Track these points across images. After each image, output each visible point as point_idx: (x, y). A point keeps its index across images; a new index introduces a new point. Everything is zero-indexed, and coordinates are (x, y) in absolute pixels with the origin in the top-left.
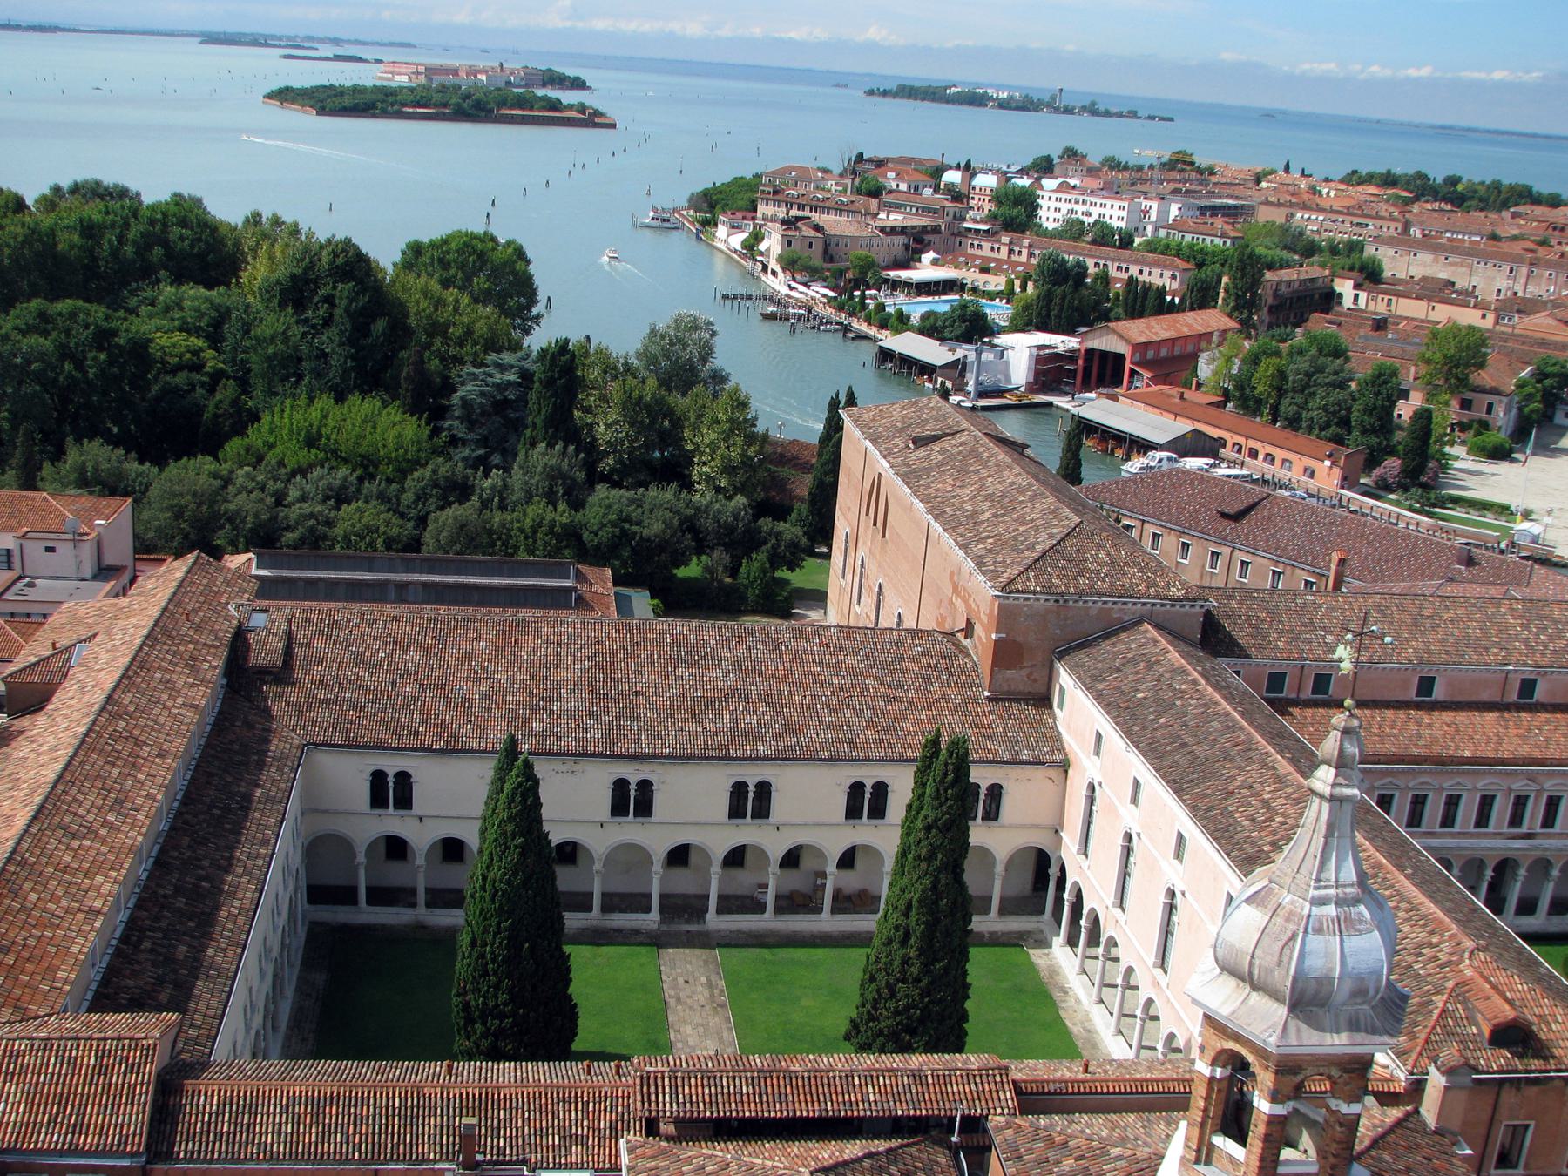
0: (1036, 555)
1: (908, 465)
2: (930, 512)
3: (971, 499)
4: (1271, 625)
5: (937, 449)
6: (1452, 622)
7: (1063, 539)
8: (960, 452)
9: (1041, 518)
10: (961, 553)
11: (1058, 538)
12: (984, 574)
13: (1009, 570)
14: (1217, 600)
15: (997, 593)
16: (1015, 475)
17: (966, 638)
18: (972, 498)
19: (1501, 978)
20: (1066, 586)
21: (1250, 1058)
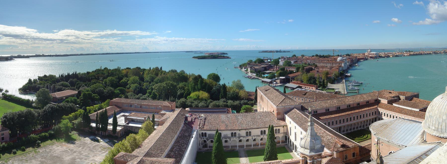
0: (280, 102)
2: (268, 98)
7: (284, 100)
10: (272, 103)
19: (341, 140)
21: (306, 156)
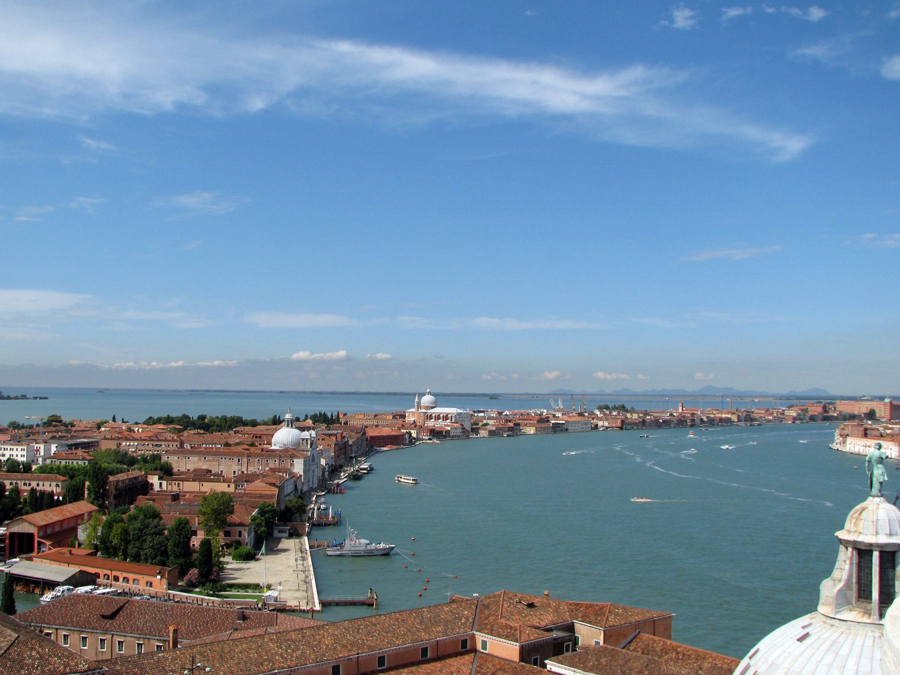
6: (241, 652)
7: (8, 649)
11: (5, 648)
14: (107, 667)
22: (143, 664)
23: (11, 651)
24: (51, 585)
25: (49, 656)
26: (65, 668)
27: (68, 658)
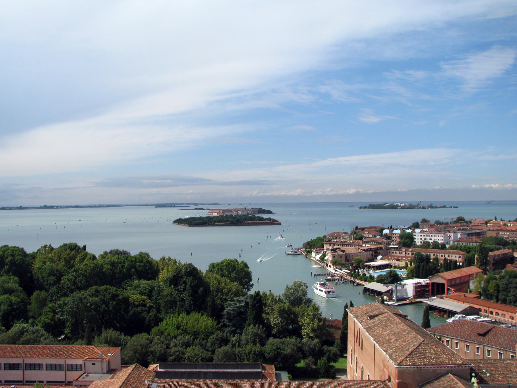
0: (409, 352)
1: (368, 325)
2: (374, 340)
3: (388, 335)
4: (495, 372)
5: (377, 319)
7: (418, 346)
8: (384, 320)
9: (411, 340)
10: (385, 353)
11: (417, 346)
12: (392, 360)
13: (400, 358)
14: (475, 364)
15: (396, 366)
16: (402, 326)
17: (389, 382)
18: (388, 335)
20: (420, 362)
22: (497, 365)
23: (420, 348)
24: (452, 313)
25: (441, 353)
26: (449, 361)
27: (451, 356)
